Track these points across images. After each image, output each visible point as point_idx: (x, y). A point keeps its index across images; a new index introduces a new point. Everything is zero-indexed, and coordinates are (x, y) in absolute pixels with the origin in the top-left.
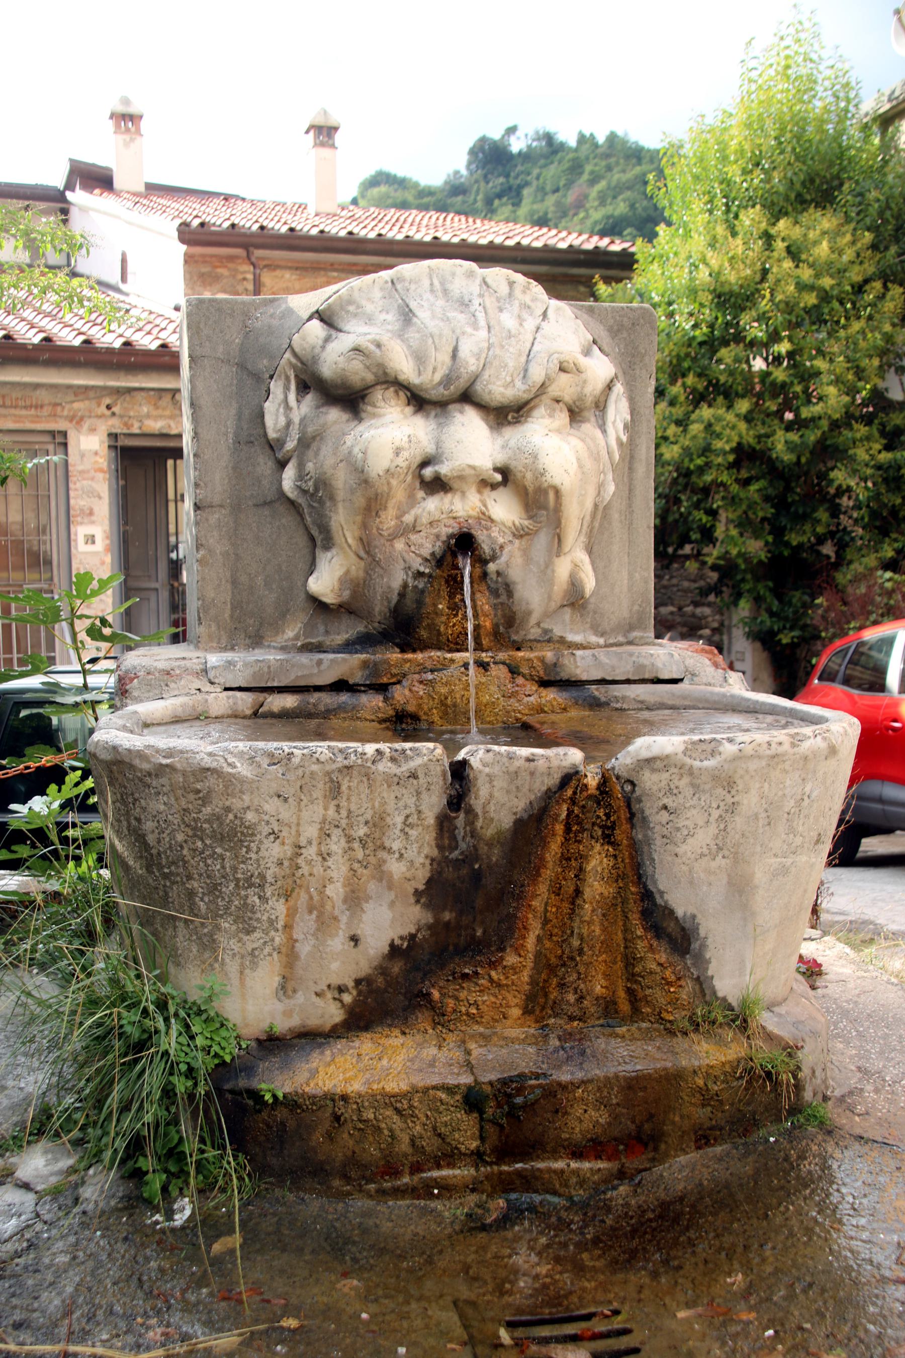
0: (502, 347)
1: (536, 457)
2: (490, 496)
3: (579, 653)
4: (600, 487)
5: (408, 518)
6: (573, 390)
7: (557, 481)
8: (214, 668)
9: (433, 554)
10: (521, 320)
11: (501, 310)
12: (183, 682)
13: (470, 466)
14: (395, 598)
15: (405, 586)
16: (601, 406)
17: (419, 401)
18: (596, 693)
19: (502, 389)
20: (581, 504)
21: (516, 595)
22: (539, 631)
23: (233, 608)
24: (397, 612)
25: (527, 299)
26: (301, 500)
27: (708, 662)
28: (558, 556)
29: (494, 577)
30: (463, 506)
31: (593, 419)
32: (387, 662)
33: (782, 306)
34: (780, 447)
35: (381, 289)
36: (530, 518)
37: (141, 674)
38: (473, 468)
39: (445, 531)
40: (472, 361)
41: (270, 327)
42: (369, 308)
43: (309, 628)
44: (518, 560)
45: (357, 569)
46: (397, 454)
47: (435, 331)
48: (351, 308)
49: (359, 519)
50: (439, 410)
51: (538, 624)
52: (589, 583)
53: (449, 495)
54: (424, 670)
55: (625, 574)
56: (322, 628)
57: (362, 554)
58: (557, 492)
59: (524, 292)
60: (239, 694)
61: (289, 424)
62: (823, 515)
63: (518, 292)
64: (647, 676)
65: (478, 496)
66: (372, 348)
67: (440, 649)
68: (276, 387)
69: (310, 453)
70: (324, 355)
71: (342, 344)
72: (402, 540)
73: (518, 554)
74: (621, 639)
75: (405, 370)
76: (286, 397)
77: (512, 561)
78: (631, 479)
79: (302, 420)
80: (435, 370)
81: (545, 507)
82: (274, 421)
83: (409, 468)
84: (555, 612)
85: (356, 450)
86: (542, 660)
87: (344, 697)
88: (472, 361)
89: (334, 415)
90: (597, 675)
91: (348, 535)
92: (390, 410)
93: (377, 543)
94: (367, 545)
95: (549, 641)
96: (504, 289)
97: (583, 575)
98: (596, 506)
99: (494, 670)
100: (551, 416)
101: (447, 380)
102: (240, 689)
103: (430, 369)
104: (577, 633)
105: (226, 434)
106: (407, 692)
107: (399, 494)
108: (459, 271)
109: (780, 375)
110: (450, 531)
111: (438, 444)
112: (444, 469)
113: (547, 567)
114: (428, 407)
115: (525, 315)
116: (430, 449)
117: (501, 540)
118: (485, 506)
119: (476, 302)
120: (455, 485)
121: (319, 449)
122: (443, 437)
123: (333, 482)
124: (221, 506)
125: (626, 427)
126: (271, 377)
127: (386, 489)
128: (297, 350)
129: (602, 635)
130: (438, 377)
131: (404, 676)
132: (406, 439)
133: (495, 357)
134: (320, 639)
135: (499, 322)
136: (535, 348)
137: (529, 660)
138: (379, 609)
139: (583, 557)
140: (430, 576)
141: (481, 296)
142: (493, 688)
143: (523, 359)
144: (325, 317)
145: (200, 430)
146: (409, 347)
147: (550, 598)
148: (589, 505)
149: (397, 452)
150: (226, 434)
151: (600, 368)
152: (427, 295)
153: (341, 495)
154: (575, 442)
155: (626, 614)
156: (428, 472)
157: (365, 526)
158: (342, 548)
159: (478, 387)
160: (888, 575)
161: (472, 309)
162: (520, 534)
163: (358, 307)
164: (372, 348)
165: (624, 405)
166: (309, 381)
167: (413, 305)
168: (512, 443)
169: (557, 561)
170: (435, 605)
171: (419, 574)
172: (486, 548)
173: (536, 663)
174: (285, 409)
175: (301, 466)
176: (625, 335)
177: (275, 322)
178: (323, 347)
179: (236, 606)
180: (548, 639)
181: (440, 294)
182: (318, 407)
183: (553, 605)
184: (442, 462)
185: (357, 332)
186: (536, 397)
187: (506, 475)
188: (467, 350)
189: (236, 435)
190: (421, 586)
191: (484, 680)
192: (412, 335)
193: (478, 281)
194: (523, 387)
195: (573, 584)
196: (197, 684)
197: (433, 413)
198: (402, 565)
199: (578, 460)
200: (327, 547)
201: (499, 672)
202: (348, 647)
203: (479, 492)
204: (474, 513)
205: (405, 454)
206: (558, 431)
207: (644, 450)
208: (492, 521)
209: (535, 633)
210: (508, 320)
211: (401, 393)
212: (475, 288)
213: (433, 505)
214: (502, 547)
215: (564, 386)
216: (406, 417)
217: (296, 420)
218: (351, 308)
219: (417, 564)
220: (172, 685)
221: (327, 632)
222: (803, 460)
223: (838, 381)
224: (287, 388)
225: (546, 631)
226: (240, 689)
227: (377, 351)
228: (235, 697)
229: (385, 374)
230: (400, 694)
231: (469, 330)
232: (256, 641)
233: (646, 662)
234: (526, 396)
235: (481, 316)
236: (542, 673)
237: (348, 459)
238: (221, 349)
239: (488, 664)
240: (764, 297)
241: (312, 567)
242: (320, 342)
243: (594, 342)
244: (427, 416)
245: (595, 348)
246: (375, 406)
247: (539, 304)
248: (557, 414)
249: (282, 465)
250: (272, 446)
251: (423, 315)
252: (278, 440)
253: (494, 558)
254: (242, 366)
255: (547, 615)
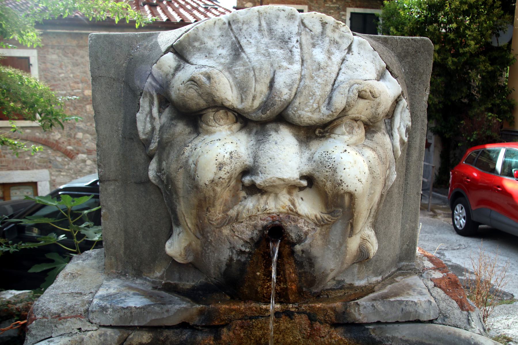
0: (312, 78)
1: (334, 170)
2: (297, 197)
3: (362, 301)
4: (387, 179)
5: (232, 213)
6: (368, 111)
7: (351, 189)
8: (92, 312)
9: (252, 239)
10: (330, 53)
11: (314, 46)
12: (67, 324)
13: (279, 179)
14: (224, 267)
15: (231, 259)
16: (390, 116)
17: (243, 120)
18: (373, 334)
19: (309, 114)
20: (370, 200)
21: (317, 266)
22: (334, 282)
23: (126, 248)
24: (226, 274)
25: (336, 36)
26: (160, 186)
27: (455, 305)
28: (351, 236)
29: (300, 254)
30: (276, 205)
31: (383, 127)
32: (217, 311)
33: (454, 10)
34: (450, 63)
35: (220, 29)
36: (329, 213)
37: (39, 316)
38: (283, 180)
39: (261, 223)
40: (285, 91)
41: (143, 56)
42: (210, 44)
43: (169, 272)
44: (319, 242)
45: (196, 244)
46: (220, 169)
47: (257, 65)
48: (197, 44)
49: (194, 212)
50: (259, 127)
51: (334, 279)
52: (373, 247)
53: (265, 197)
54: (245, 317)
55: (399, 227)
56: (177, 275)
57: (198, 235)
58: (352, 196)
59: (334, 31)
60: (109, 331)
61: (153, 129)
62: (465, 89)
63: (329, 31)
64: (411, 319)
65: (288, 196)
66: (204, 79)
67: (257, 300)
68: (144, 103)
69: (165, 155)
70: (173, 81)
71: (189, 71)
72: (228, 227)
73: (318, 236)
74: (393, 270)
75: (230, 98)
76: (151, 110)
77: (314, 243)
78: (408, 161)
79: (161, 127)
80: (254, 98)
81: (342, 206)
82: (143, 126)
83: (230, 178)
84: (346, 269)
85: (191, 161)
86: (334, 309)
87: (186, 335)
88: (285, 91)
89: (181, 128)
90: (374, 319)
91: (188, 221)
92: (221, 128)
93: (208, 229)
94: (202, 230)
95: (341, 288)
96: (318, 29)
97: (369, 245)
98: (382, 195)
99: (298, 318)
100: (350, 133)
101: (265, 106)
102: (111, 327)
103: (250, 97)
104: (363, 279)
105: (117, 131)
106: (231, 334)
107: (224, 194)
108: (282, 14)
109: (452, 36)
110: (265, 223)
111: (256, 158)
112: (259, 180)
113: (341, 245)
114: (252, 125)
115: (334, 50)
116: (249, 161)
117: (306, 229)
118: (293, 204)
119: (294, 39)
120: (269, 190)
121: (169, 154)
122: (260, 153)
123: (176, 182)
124: (115, 180)
125: (408, 130)
126: (141, 94)
127: (212, 193)
128: (155, 76)
129: (380, 275)
130: (257, 104)
131: (231, 321)
132: (227, 156)
133: (305, 87)
134: (176, 282)
135: (311, 56)
136: (340, 78)
137: (324, 310)
138: (214, 273)
139: (370, 233)
140: (250, 253)
141: (299, 34)
142: (296, 332)
143: (329, 88)
144: (180, 51)
145: (99, 129)
146: (235, 78)
147: (343, 263)
148: (377, 198)
149: (220, 166)
150: (117, 131)
151: (390, 88)
152: (256, 34)
153: (181, 192)
154: (369, 153)
155: (398, 252)
156: (247, 180)
157: (199, 217)
158: (186, 229)
159: (290, 112)
160: (490, 114)
161: (290, 45)
162: (319, 223)
163: (202, 43)
164: (204, 79)
165: (407, 114)
166: (165, 100)
167: (243, 42)
168: (316, 157)
169: (349, 240)
170: (255, 273)
171: (241, 252)
172: (293, 235)
173: (330, 312)
174: (148, 118)
175: (160, 162)
176: (409, 59)
177: (146, 53)
178: (174, 75)
179: (127, 247)
180: (341, 286)
181: (266, 33)
182: (172, 119)
183: (345, 266)
184: (257, 174)
185: (199, 65)
186: (338, 118)
187: (310, 180)
188: (281, 81)
189: (124, 132)
190: (243, 260)
191: (289, 326)
192: (239, 68)
193: (297, 22)
194: (327, 113)
195: (361, 251)
196: (79, 325)
197: (255, 130)
198: (228, 245)
199: (370, 168)
200: (178, 225)
201: (302, 320)
202: (192, 295)
203: (290, 193)
204: (284, 210)
205: (227, 168)
206: (356, 145)
207: (418, 141)
208: (299, 215)
209: (330, 284)
210: (319, 54)
211: (230, 114)
212: (294, 28)
213: (251, 204)
214: (306, 234)
215: (362, 110)
216: (233, 133)
217: (158, 127)
218: (197, 44)
219: (239, 245)
220: (60, 326)
221: (180, 279)
222: (459, 68)
223: (474, 39)
224: (151, 104)
225: (339, 282)
226: (111, 327)
227: (207, 83)
228: (105, 334)
229: (214, 101)
230: (226, 334)
231: (285, 64)
232: (138, 274)
233: (411, 309)
234: (329, 119)
235: (297, 51)
236: (333, 319)
237: (185, 165)
238: (113, 71)
239: (293, 313)
240: (447, 6)
241: (169, 235)
242: (172, 71)
243: (387, 68)
244: (249, 133)
245: (388, 73)
246: (208, 125)
247: (345, 40)
248: (356, 129)
249: (151, 158)
250: (146, 144)
251: (250, 50)
252: (146, 140)
253: (300, 241)
254: (126, 83)
255: (339, 272)
